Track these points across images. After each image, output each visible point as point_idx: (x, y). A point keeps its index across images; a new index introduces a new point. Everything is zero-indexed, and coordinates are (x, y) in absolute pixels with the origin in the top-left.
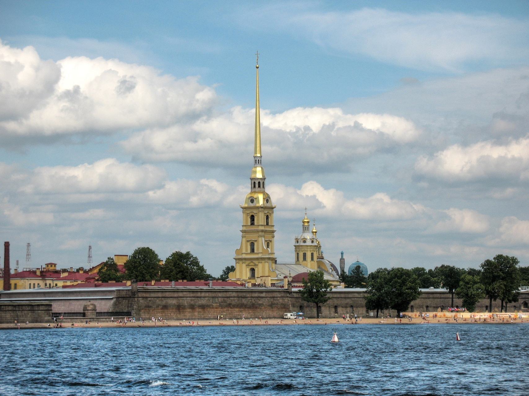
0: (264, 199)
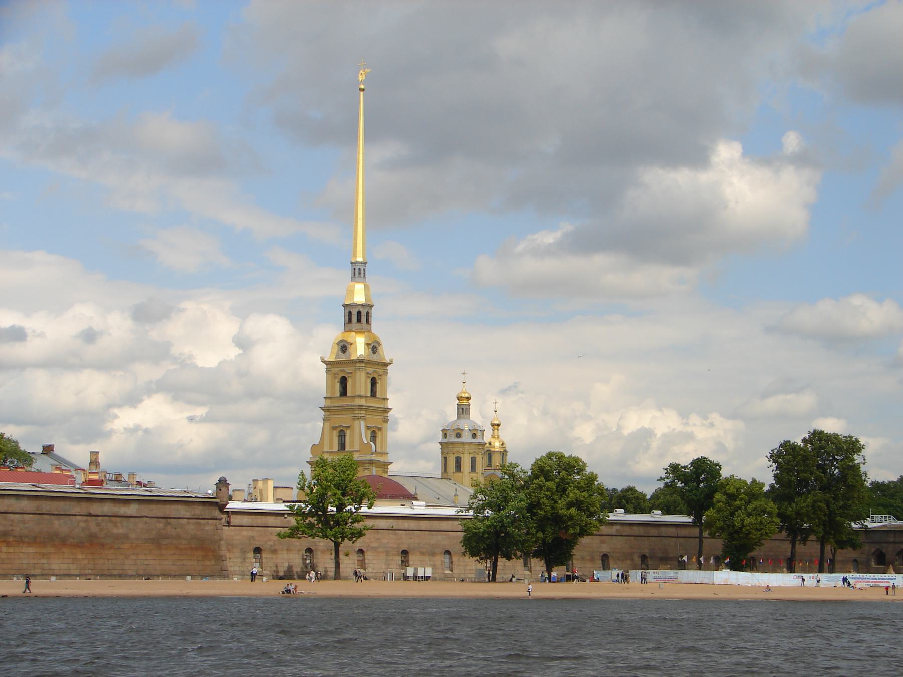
0: (367, 344)
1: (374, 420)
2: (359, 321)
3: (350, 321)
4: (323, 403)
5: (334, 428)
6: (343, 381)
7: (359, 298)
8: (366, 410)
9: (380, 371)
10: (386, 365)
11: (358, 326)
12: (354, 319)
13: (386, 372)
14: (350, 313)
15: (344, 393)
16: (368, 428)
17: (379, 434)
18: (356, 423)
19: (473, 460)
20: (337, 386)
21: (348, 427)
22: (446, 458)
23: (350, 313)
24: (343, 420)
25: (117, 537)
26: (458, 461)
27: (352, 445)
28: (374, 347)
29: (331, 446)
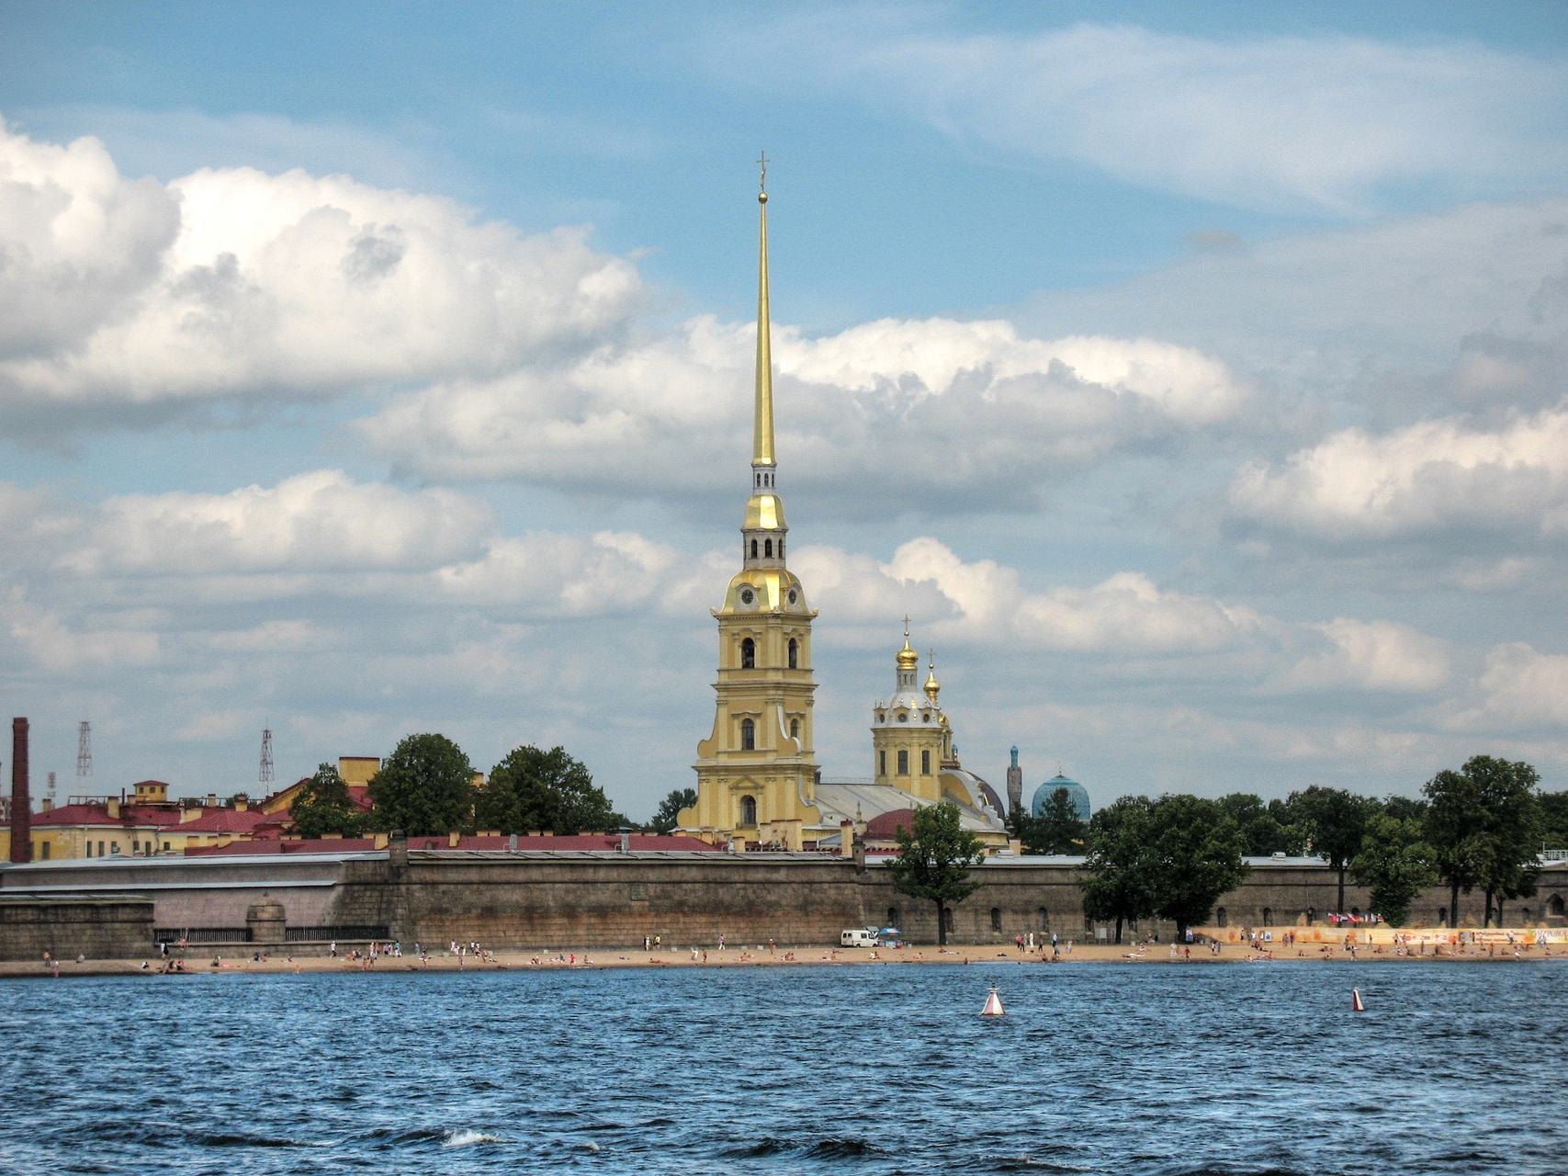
0: (782, 590)
1: (795, 703)
2: (768, 554)
3: (755, 554)
4: (715, 678)
5: (735, 716)
6: (748, 647)
7: (768, 520)
8: (785, 689)
9: (802, 629)
10: (807, 618)
11: (768, 562)
12: (761, 551)
13: (809, 631)
14: (755, 542)
15: (748, 664)
16: (788, 715)
17: (801, 724)
18: (771, 709)
19: (926, 755)
20: (739, 652)
21: (758, 715)
22: (883, 753)
23: (755, 542)
24: (749, 704)
25: (771, 905)
26: (903, 757)
27: (764, 739)
28: (792, 591)
29: (731, 743)
